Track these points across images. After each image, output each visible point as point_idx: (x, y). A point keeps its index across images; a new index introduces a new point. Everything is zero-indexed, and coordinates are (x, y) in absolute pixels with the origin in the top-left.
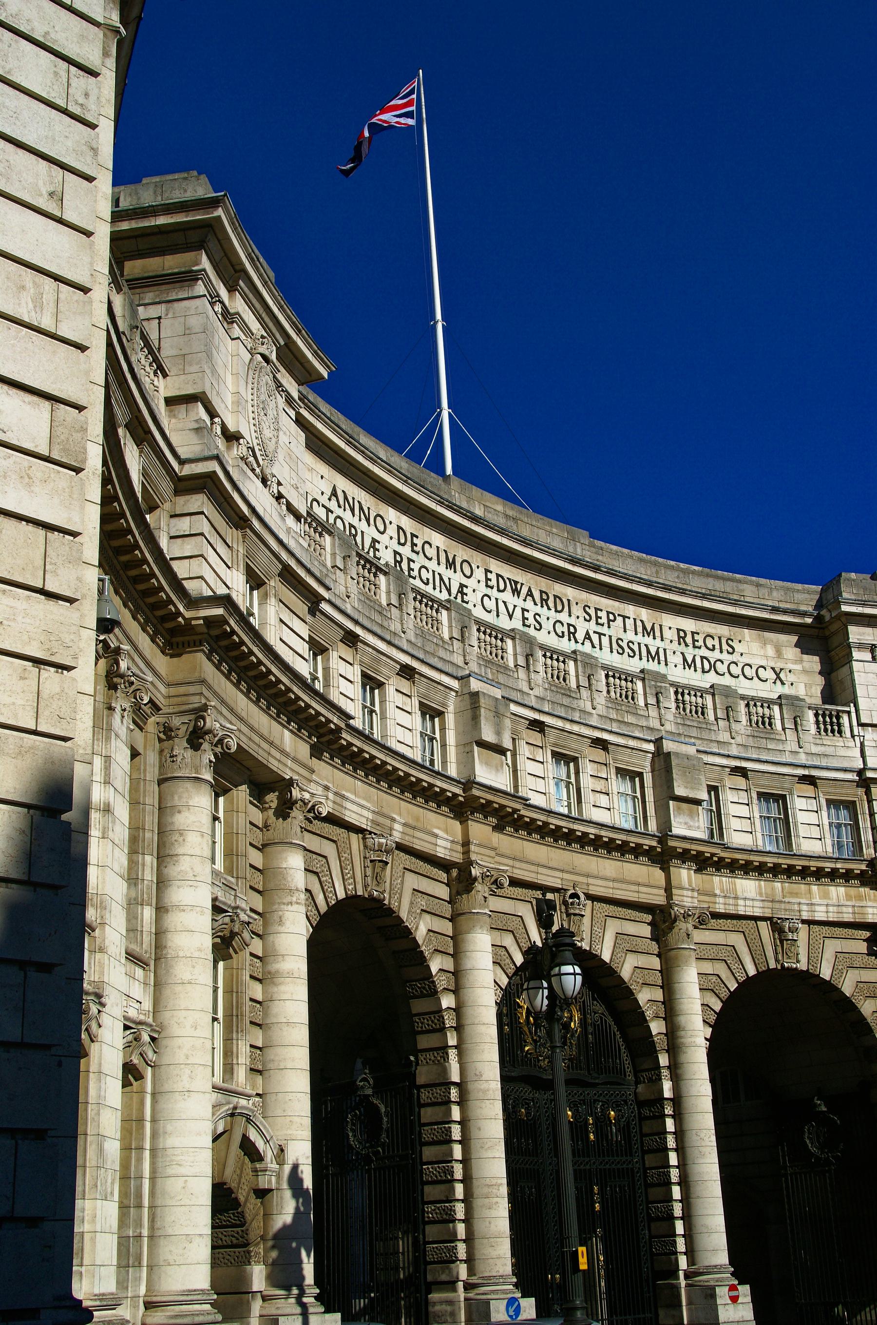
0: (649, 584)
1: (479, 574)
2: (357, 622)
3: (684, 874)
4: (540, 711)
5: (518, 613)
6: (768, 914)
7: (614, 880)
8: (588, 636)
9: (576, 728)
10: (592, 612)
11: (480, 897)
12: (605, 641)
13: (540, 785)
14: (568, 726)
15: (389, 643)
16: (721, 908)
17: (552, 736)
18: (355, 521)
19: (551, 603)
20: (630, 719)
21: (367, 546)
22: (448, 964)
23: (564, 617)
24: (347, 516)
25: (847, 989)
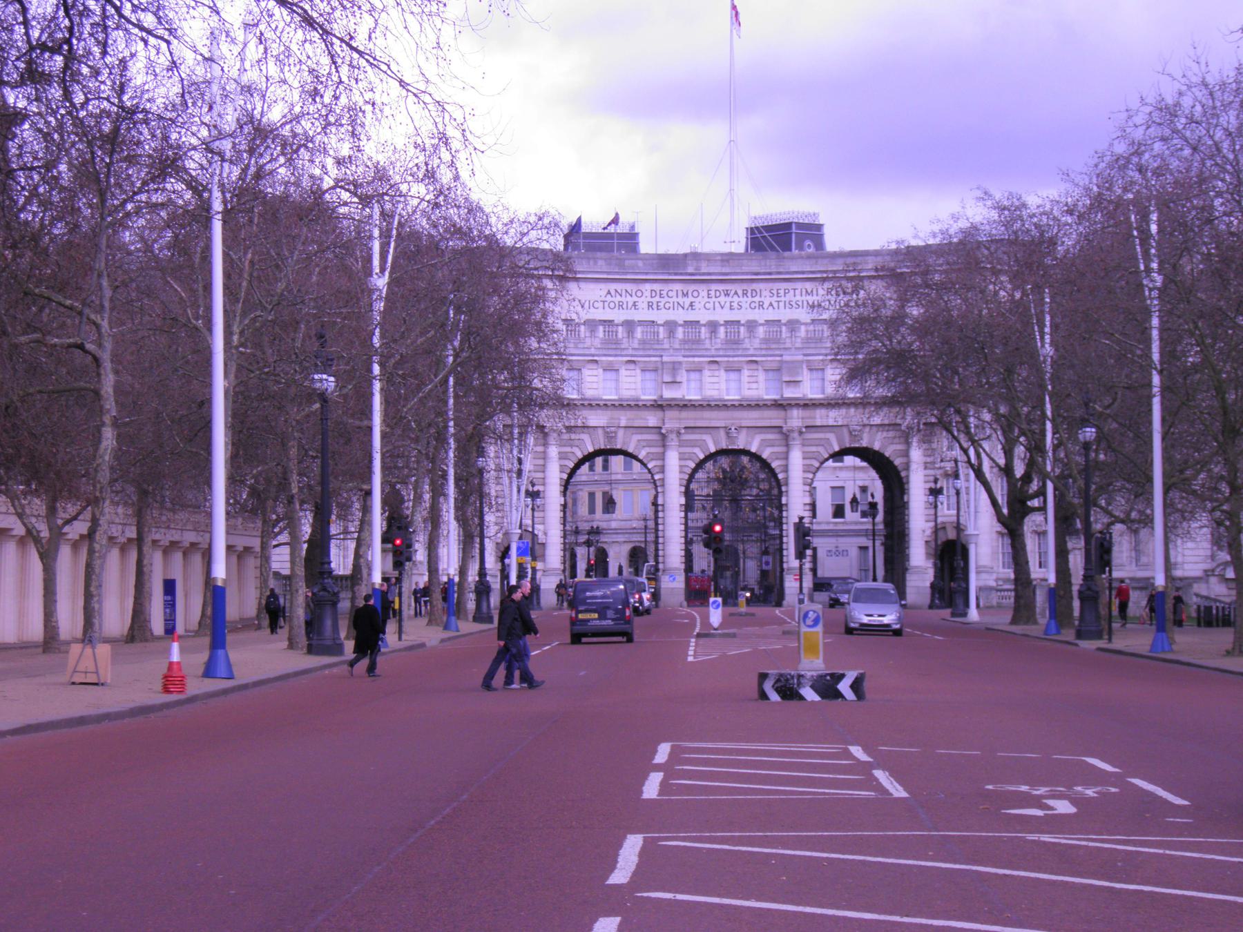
0: (803, 273)
1: (704, 294)
2: (593, 356)
3: (795, 412)
4: (713, 356)
5: (728, 305)
6: (845, 423)
7: (756, 419)
8: (771, 304)
9: (736, 359)
10: (775, 292)
11: (669, 439)
12: (782, 304)
13: (716, 386)
14: (731, 359)
15: (616, 356)
16: (818, 423)
17: (723, 365)
18: (623, 299)
19: (749, 294)
20: (774, 346)
21: (630, 305)
22: (659, 463)
23: (757, 299)
24: (619, 298)
25: (887, 454)
